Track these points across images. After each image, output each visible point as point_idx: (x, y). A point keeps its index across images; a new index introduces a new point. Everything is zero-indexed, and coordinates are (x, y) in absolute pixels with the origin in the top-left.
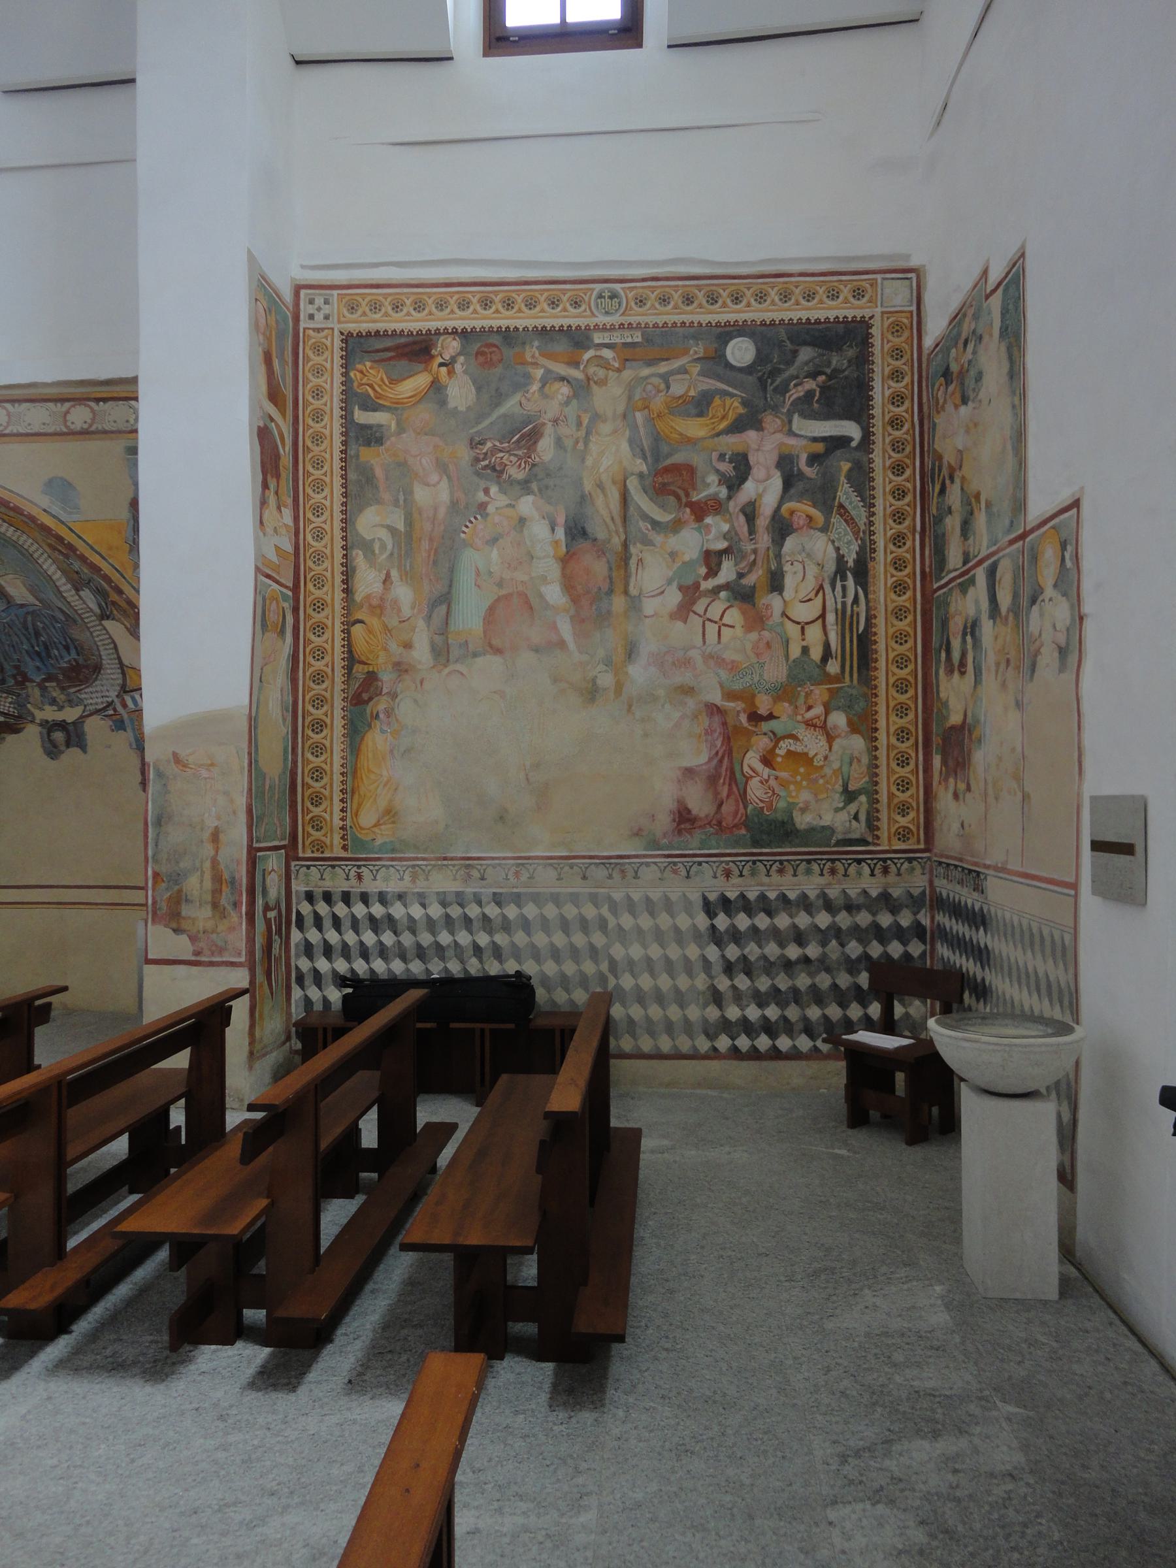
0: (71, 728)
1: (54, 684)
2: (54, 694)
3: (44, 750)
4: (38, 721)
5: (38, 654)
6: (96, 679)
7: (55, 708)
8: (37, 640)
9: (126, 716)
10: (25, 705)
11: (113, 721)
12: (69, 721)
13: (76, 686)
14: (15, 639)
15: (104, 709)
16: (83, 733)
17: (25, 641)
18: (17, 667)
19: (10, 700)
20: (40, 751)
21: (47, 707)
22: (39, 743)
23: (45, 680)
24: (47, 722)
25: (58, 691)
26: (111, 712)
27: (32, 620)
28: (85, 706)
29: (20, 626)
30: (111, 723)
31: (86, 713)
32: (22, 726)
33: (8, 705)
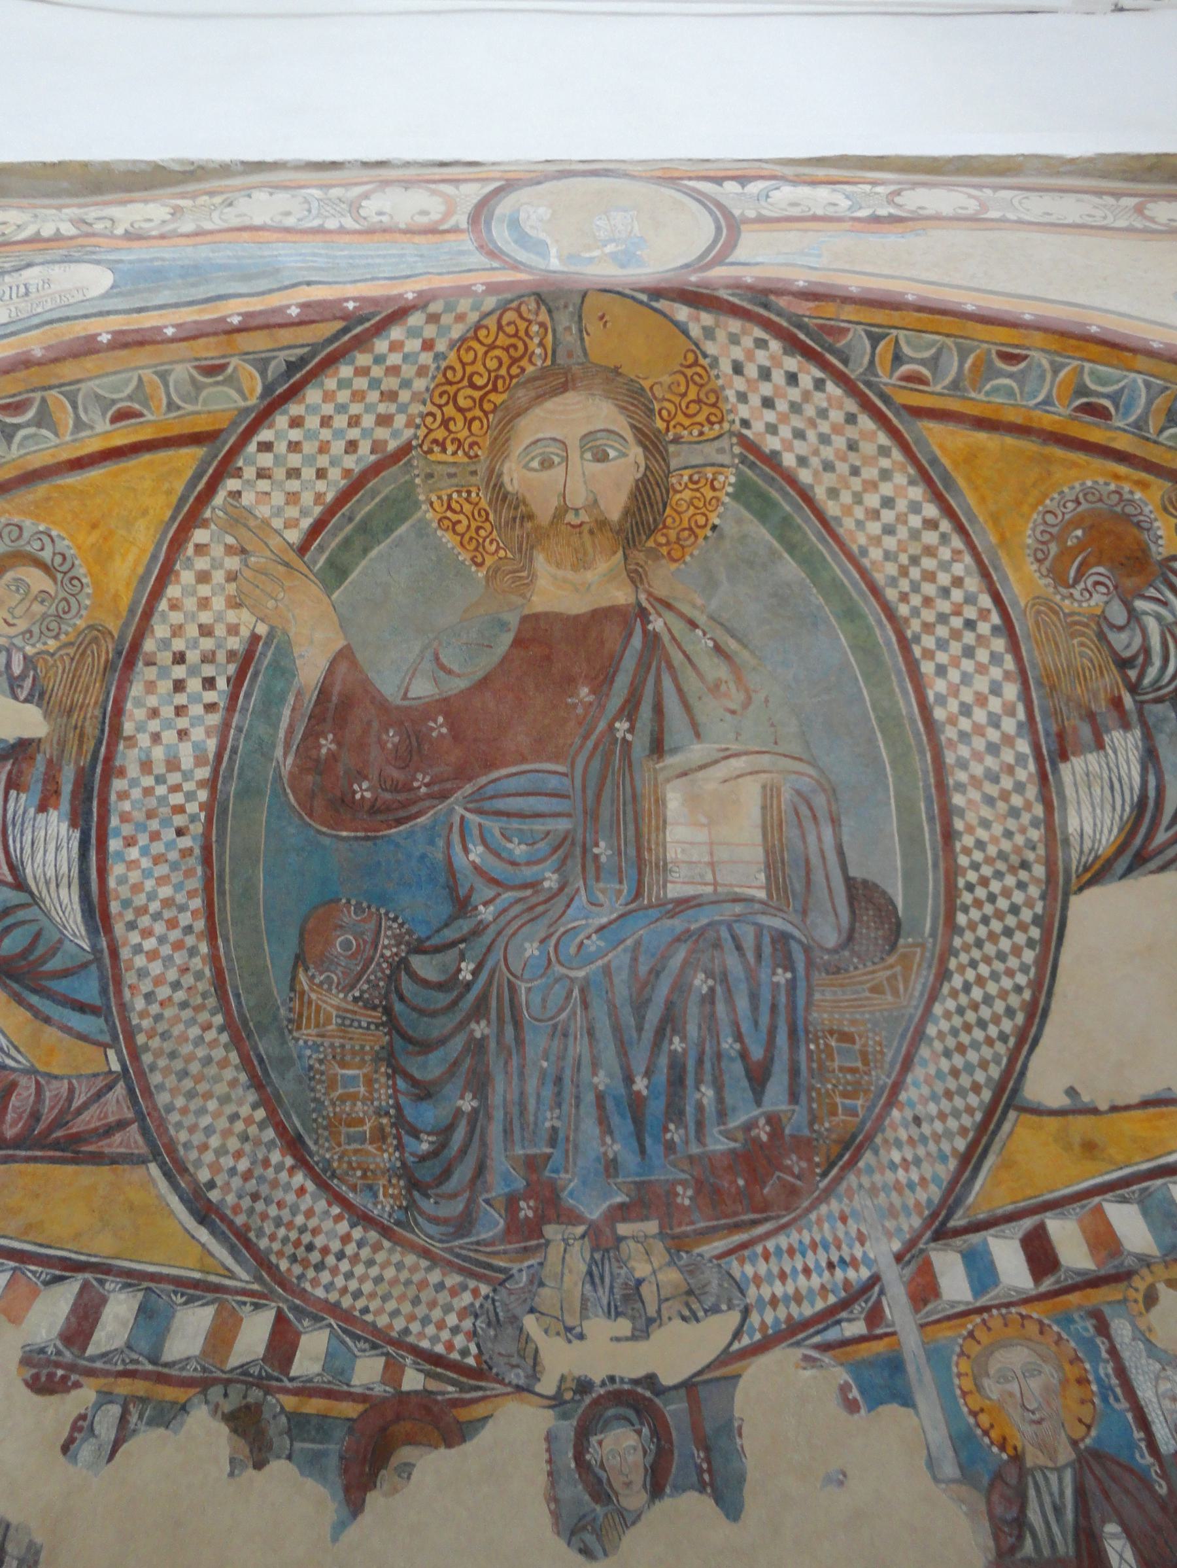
0: (674, 1409)
1: (652, 1227)
2: (642, 1269)
3: (556, 1516)
4: (547, 1386)
5: (636, 1106)
6: (828, 1193)
7: (624, 1326)
8: (657, 1044)
9: (911, 1341)
10: (515, 1320)
11: (856, 1368)
12: (668, 1379)
13: (738, 1227)
14: (579, 1047)
15: (829, 1315)
16: (729, 1429)
17: (609, 1055)
18: (532, 1165)
19: (466, 1298)
20: (539, 1516)
21: (600, 1328)
22: (542, 1479)
23: (622, 1212)
24: (584, 1386)
25: (659, 1247)
26: (856, 1328)
27: (686, 963)
28: (746, 1312)
29: (622, 991)
30: (843, 1376)
31: (746, 1341)
32: (479, 1410)
33: (452, 1320)
